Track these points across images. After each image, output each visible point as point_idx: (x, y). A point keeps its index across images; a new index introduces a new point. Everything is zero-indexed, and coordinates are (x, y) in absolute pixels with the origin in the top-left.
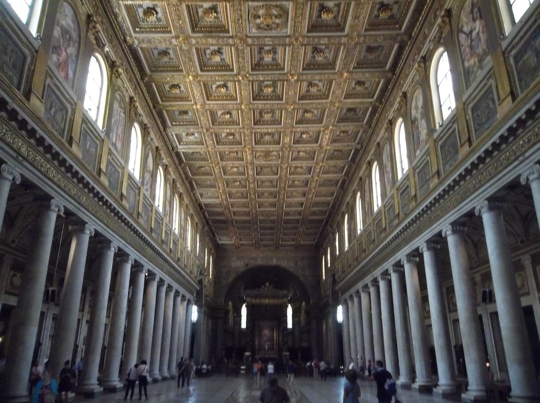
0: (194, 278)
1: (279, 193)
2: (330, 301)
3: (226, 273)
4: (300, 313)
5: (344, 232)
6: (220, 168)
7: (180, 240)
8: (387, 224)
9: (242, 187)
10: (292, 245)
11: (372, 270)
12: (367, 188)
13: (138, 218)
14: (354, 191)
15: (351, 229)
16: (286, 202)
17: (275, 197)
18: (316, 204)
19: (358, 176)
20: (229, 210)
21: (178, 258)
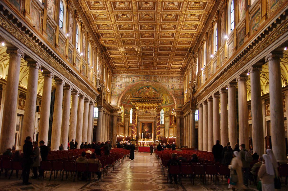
1: (156, 25)
3: (119, 86)
5: (202, 56)
6: (110, 2)
10: (166, 67)
12: (223, 19)
13: (42, 34)
14: (212, 23)
19: (216, 10)
20: (119, 39)
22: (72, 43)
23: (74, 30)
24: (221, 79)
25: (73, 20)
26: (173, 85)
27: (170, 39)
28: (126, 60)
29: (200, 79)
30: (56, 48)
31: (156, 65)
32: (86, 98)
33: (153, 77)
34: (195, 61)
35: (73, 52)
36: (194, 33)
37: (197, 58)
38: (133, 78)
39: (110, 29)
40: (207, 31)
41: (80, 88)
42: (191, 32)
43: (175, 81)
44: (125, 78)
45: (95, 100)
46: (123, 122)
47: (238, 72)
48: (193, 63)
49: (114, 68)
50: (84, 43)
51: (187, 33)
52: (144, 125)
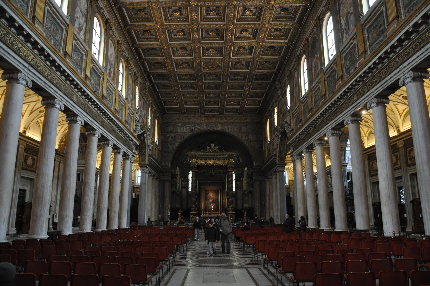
0: (132, 131)
2: (278, 161)
3: (172, 138)
4: (243, 178)
7: (106, 77)
8: (402, 9)
9: (183, 21)
10: (237, 110)
11: (355, 98)
14: (319, 17)
15: (312, 67)
16: (233, 44)
17: (222, 39)
18: (263, 65)
20: (170, 58)
21: (103, 95)
22: (85, 42)
23: (89, 21)
24: (351, 97)
25: (87, 5)
26: (247, 135)
27: (246, 59)
28: (182, 99)
29: (294, 116)
30: (34, 23)
31: (224, 106)
32: (115, 145)
33: (219, 125)
34: (283, 92)
35: (84, 56)
36: (283, 46)
37: (287, 87)
38: (192, 127)
39: (156, 39)
40: (307, 36)
41: (101, 125)
42: (280, 43)
43: (250, 130)
44: (180, 127)
45: (134, 153)
46: (178, 190)
47: (405, 64)
48: (279, 97)
49: (165, 113)
50: (111, 55)
51: (273, 45)
52: (208, 193)
